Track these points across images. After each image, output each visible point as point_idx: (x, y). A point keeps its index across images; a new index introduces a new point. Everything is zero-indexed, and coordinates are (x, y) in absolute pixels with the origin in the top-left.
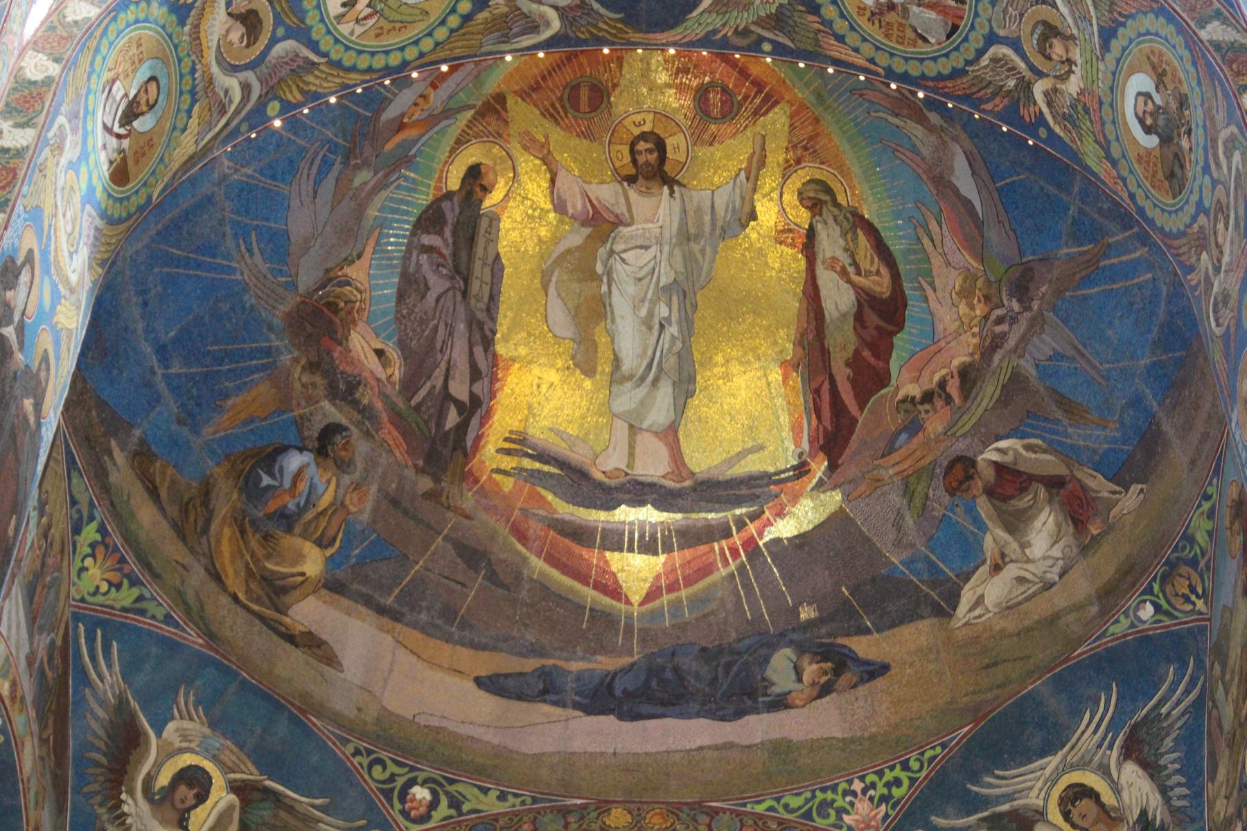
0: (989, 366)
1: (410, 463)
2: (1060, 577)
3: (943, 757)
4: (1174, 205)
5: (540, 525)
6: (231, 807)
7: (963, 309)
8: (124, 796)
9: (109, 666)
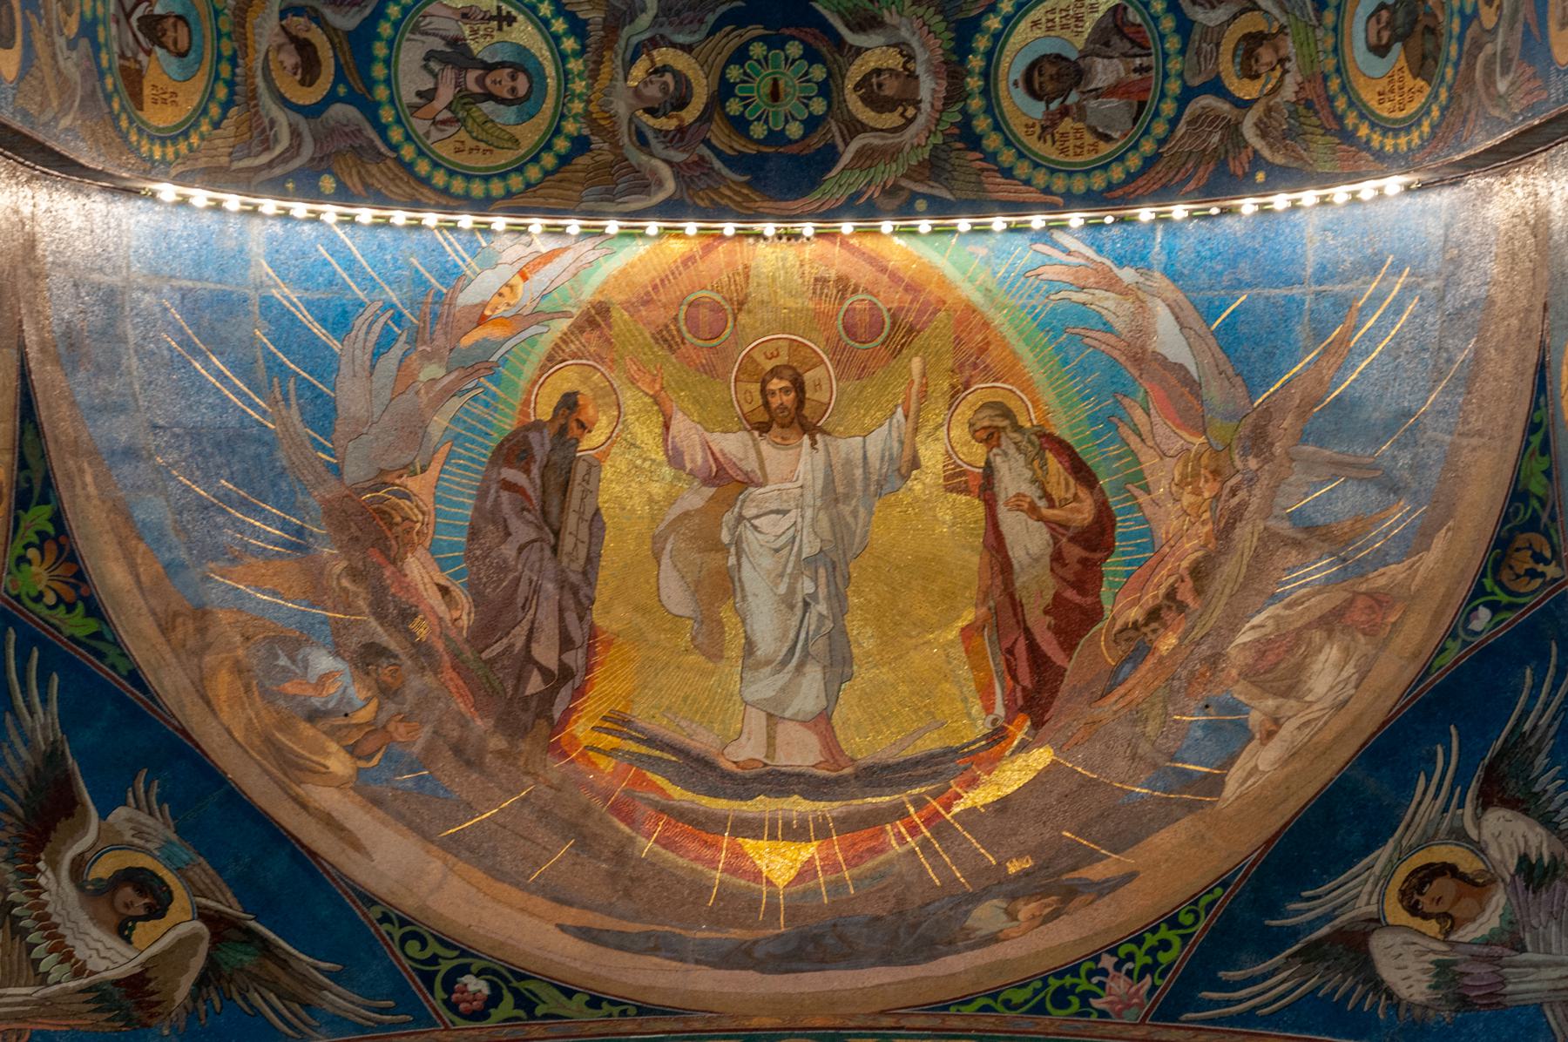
3: (1227, 897)
6: (194, 938)
7: (1187, 499)
8: (41, 865)
9: (45, 701)
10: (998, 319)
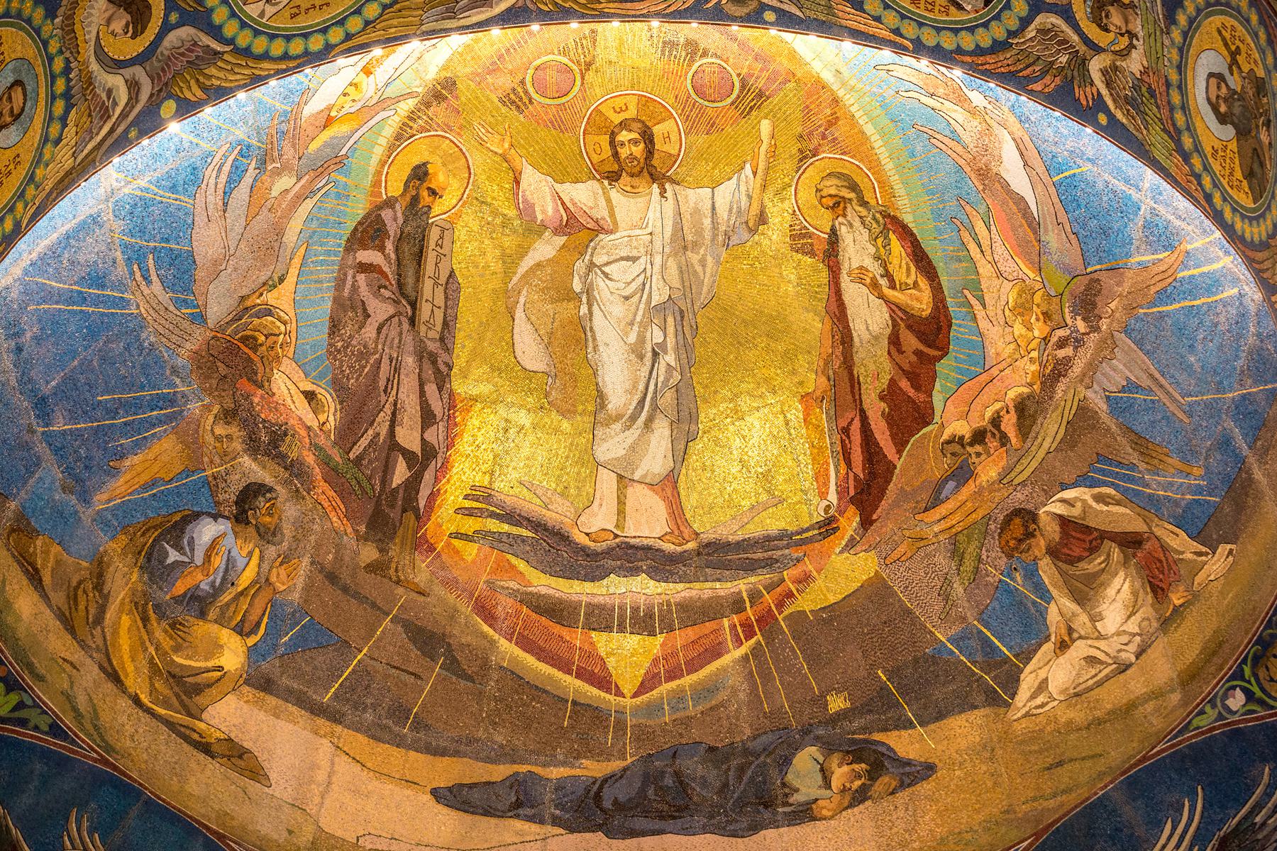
0: (1051, 398)
1: (349, 530)
2: (1137, 658)
4: (1254, 210)
5: (510, 601)
7: (1019, 329)
10: (848, 99)
